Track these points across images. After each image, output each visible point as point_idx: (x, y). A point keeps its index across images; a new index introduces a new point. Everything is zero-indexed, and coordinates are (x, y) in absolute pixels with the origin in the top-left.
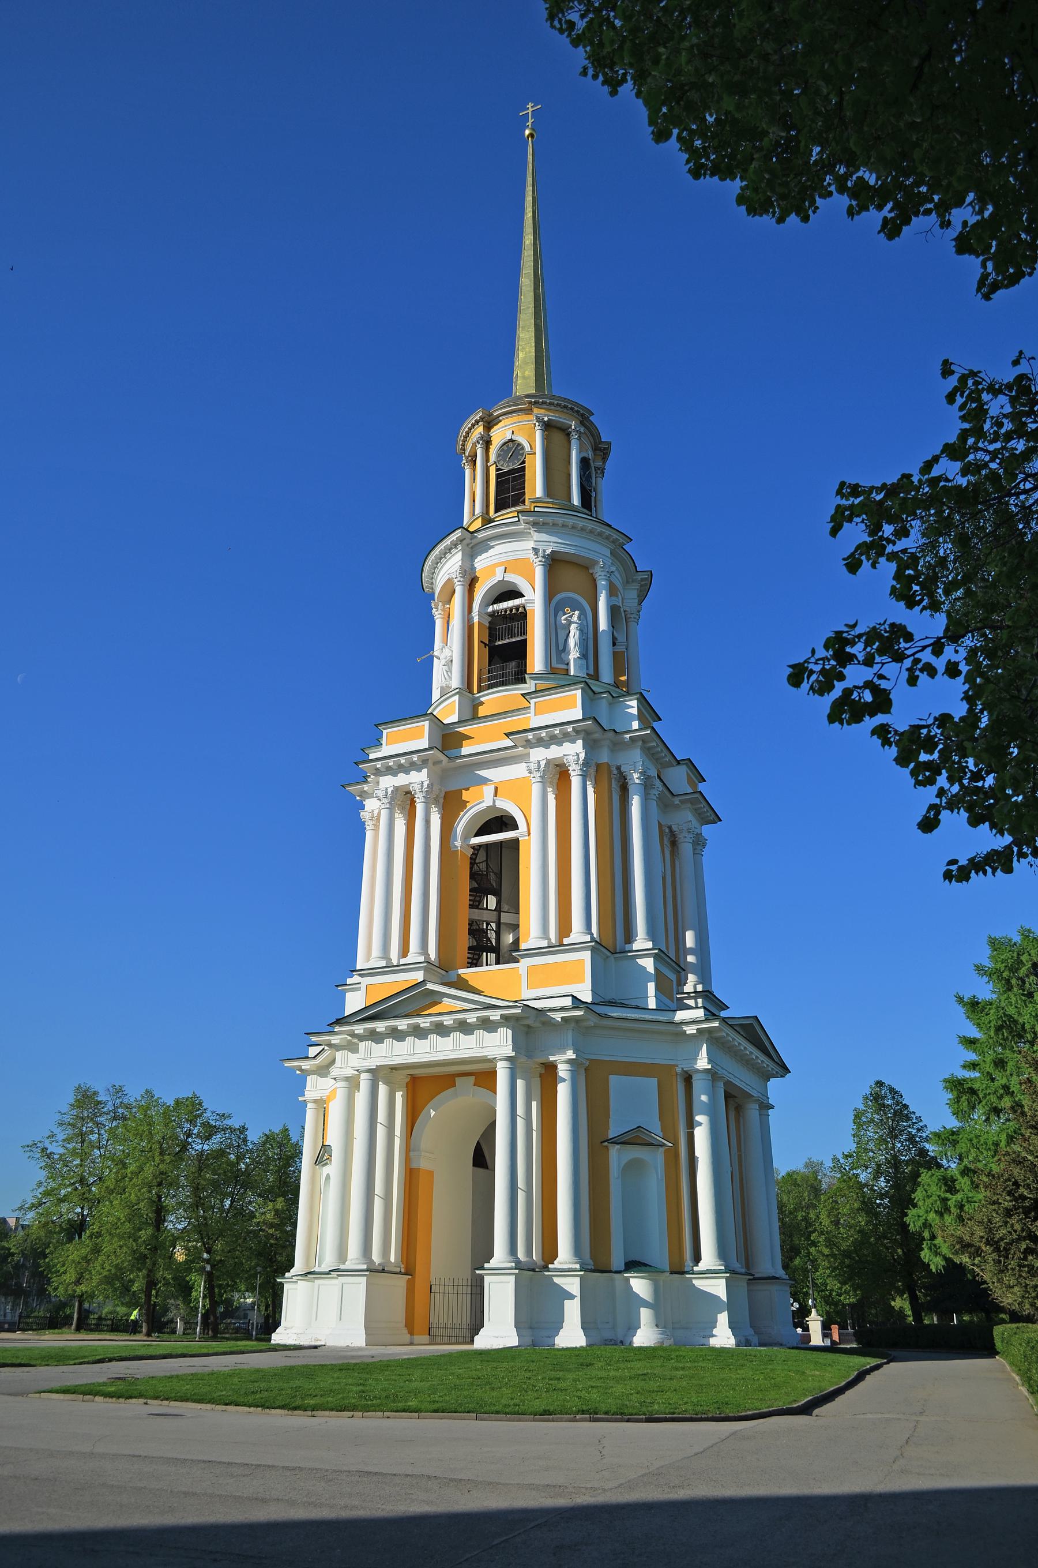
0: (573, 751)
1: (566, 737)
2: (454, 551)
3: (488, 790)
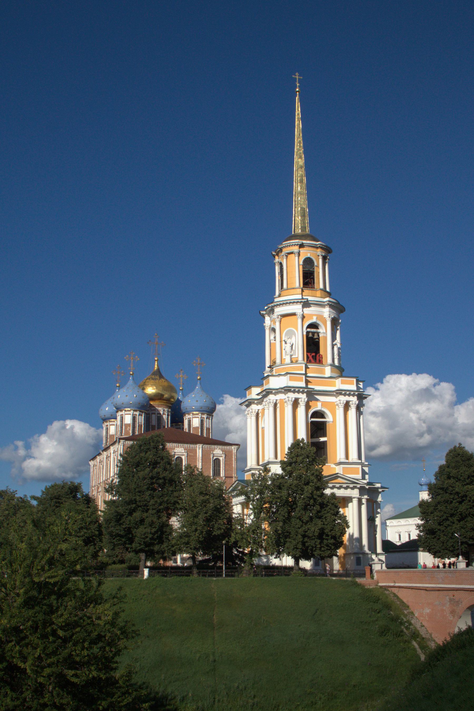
0: (354, 400)
1: (353, 395)
2: (298, 304)
3: (319, 404)
